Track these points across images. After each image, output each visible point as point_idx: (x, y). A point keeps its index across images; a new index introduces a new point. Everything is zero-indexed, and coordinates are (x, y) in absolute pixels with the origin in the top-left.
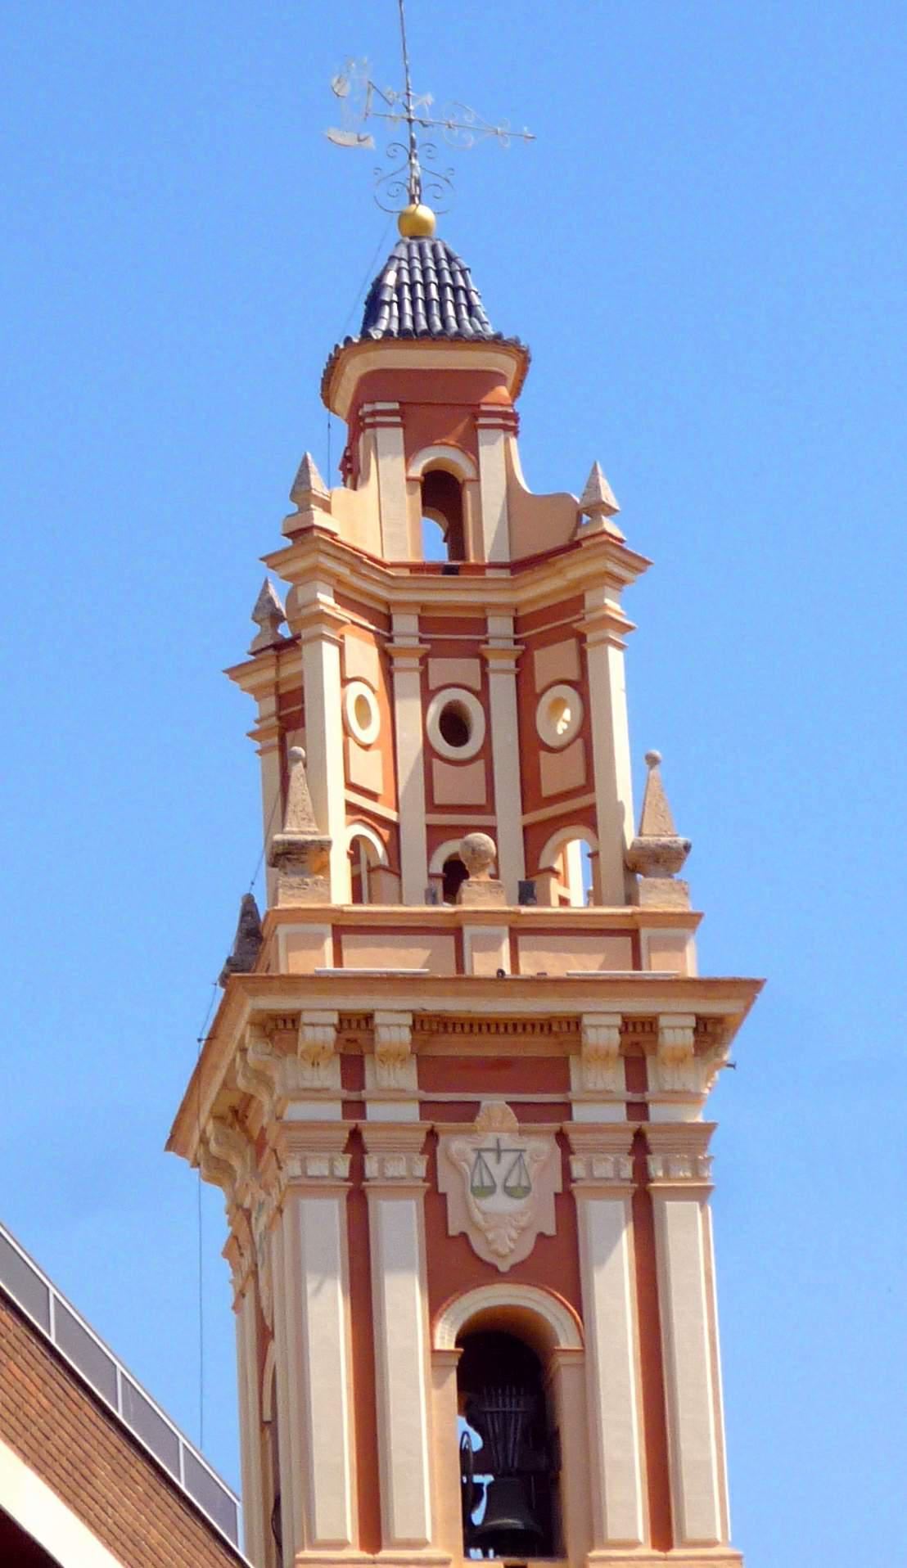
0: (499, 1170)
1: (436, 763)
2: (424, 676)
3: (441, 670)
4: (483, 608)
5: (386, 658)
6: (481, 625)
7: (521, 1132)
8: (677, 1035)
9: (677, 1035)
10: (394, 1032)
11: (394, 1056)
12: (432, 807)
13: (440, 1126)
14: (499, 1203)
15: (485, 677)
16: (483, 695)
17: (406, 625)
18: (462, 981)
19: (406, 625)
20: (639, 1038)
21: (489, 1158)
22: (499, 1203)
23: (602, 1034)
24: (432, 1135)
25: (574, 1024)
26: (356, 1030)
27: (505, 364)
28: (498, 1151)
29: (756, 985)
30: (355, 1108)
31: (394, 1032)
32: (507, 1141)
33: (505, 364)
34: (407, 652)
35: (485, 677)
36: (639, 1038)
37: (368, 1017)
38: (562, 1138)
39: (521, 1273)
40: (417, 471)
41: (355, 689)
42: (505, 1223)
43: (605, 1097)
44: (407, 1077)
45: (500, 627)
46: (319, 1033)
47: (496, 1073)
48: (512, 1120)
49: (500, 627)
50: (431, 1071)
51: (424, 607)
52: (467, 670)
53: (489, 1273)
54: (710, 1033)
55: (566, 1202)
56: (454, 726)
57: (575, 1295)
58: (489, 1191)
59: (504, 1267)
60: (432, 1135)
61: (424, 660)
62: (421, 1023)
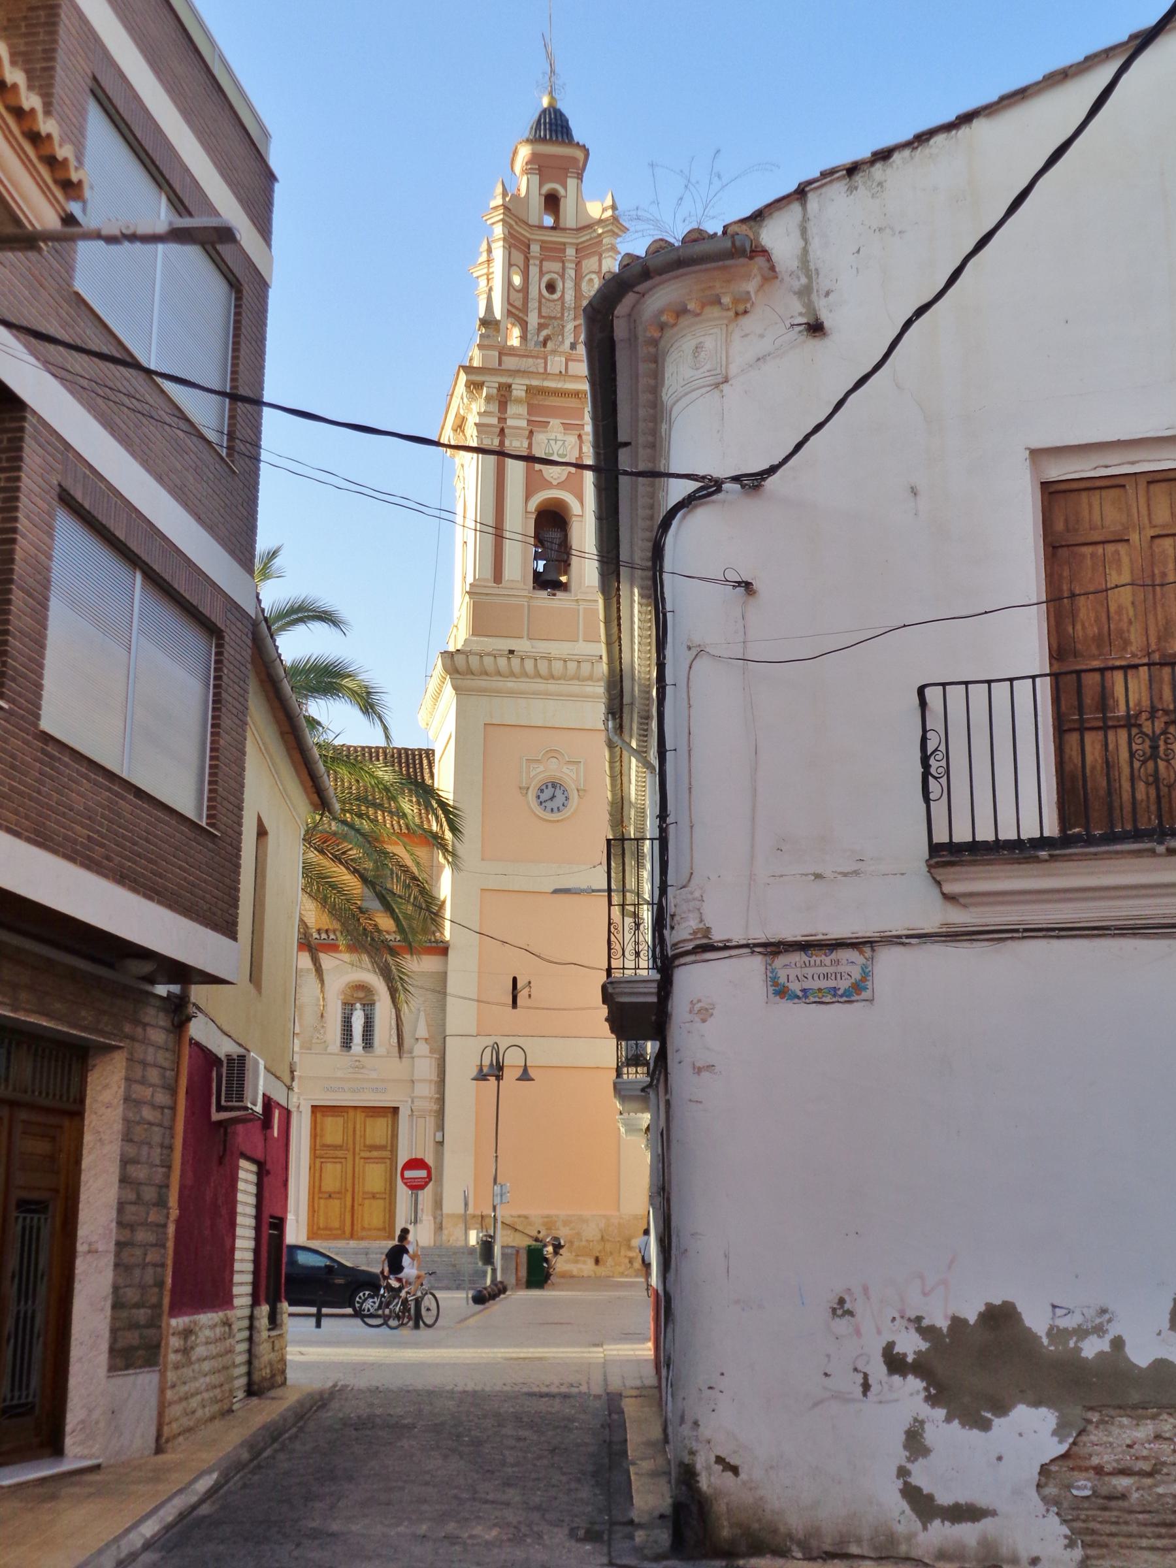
3: (547, 265)
4: (564, 244)
5: (527, 259)
6: (564, 250)
10: (518, 391)
11: (518, 401)
12: (540, 316)
16: (563, 276)
17: (535, 249)
18: (546, 374)
21: (552, 442)
24: (531, 432)
27: (580, 155)
28: (556, 440)
30: (502, 420)
32: (560, 437)
33: (580, 155)
34: (535, 258)
35: (564, 269)
37: (510, 386)
38: (580, 436)
40: (545, 190)
41: (514, 268)
44: (522, 410)
45: (571, 252)
49: (571, 252)
50: (532, 408)
51: (543, 242)
52: (556, 266)
56: (551, 287)
59: (555, 483)
60: (531, 432)
61: (541, 262)
62: (529, 389)
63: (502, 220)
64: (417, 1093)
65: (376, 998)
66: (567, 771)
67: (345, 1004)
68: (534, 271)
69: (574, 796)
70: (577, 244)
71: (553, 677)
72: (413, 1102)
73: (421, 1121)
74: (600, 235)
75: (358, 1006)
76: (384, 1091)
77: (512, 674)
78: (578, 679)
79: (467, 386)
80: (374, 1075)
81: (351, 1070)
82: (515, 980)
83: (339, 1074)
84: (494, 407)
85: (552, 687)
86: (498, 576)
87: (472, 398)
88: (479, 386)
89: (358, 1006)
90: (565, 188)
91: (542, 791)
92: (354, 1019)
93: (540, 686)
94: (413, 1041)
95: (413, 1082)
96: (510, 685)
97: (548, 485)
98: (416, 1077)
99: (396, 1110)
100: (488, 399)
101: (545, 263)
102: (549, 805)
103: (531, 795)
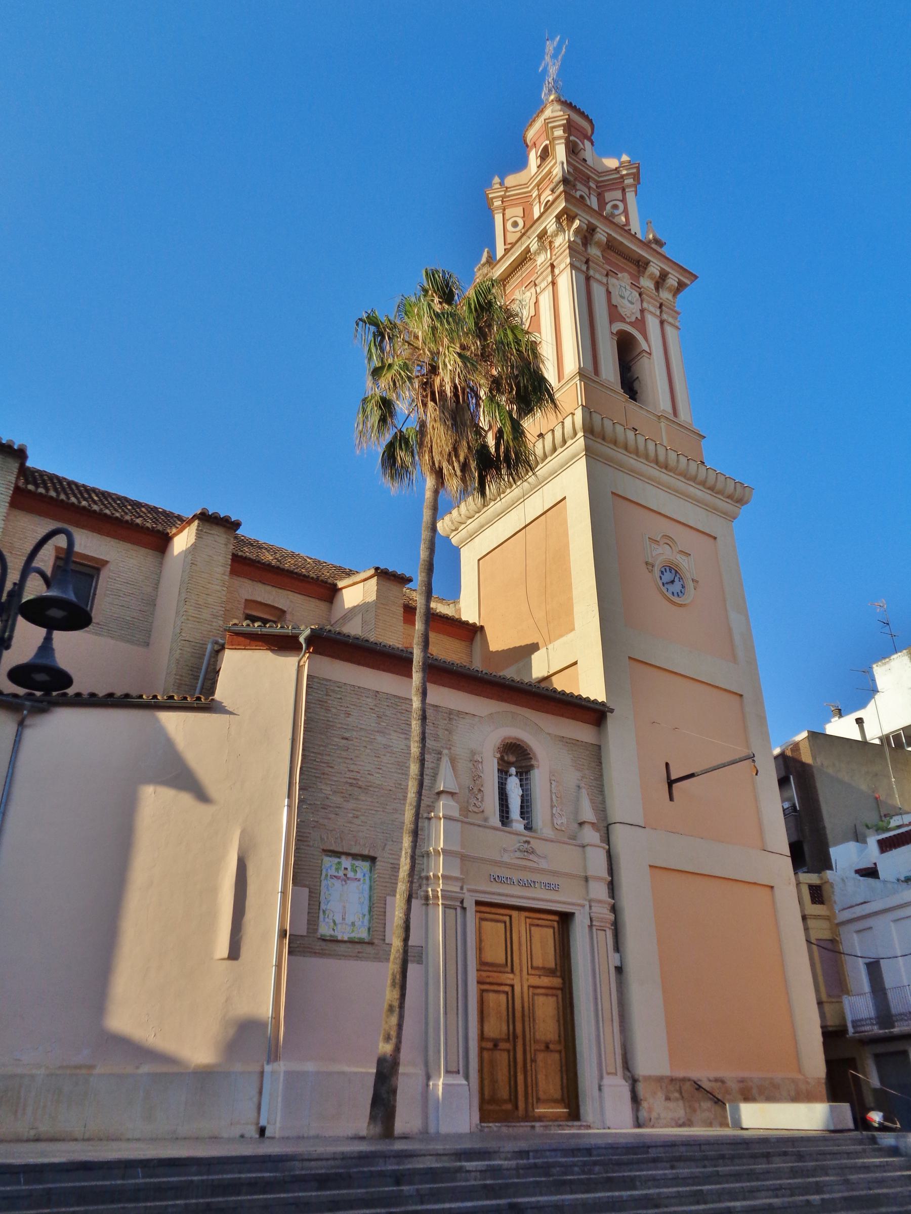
0: (626, 294)
8: (672, 281)
13: (611, 273)
20: (664, 276)
22: (626, 302)
23: (654, 269)
24: (607, 275)
25: (647, 263)
29: (696, 277)
32: (628, 287)
36: (664, 276)
38: (640, 295)
39: (630, 324)
42: (629, 307)
52: (586, 190)
53: (623, 320)
54: (681, 286)
55: (642, 311)
58: (623, 298)
62: (610, 239)
63: (563, 125)
64: (592, 895)
65: (533, 762)
69: (690, 585)
70: (598, 182)
71: (666, 468)
72: (590, 907)
73: (601, 933)
74: (622, 177)
75: (513, 770)
76: (554, 888)
77: (637, 452)
78: (685, 477)
79: (558, 217)
80: (543, 865)
81: (518, 854)
83: (506, 858)
85: (664, 477)
87: (560, 229)
88: (571, 219)
89: (513, 770)
91: (662, 573)
93: (654, 472)
94: (576, 826)
95: (586, 879)
97: (623, 320)
98: (589, 874)
99: (565, 919)
100: (577, 231)
102: (672, 588)
103: (657, 573)
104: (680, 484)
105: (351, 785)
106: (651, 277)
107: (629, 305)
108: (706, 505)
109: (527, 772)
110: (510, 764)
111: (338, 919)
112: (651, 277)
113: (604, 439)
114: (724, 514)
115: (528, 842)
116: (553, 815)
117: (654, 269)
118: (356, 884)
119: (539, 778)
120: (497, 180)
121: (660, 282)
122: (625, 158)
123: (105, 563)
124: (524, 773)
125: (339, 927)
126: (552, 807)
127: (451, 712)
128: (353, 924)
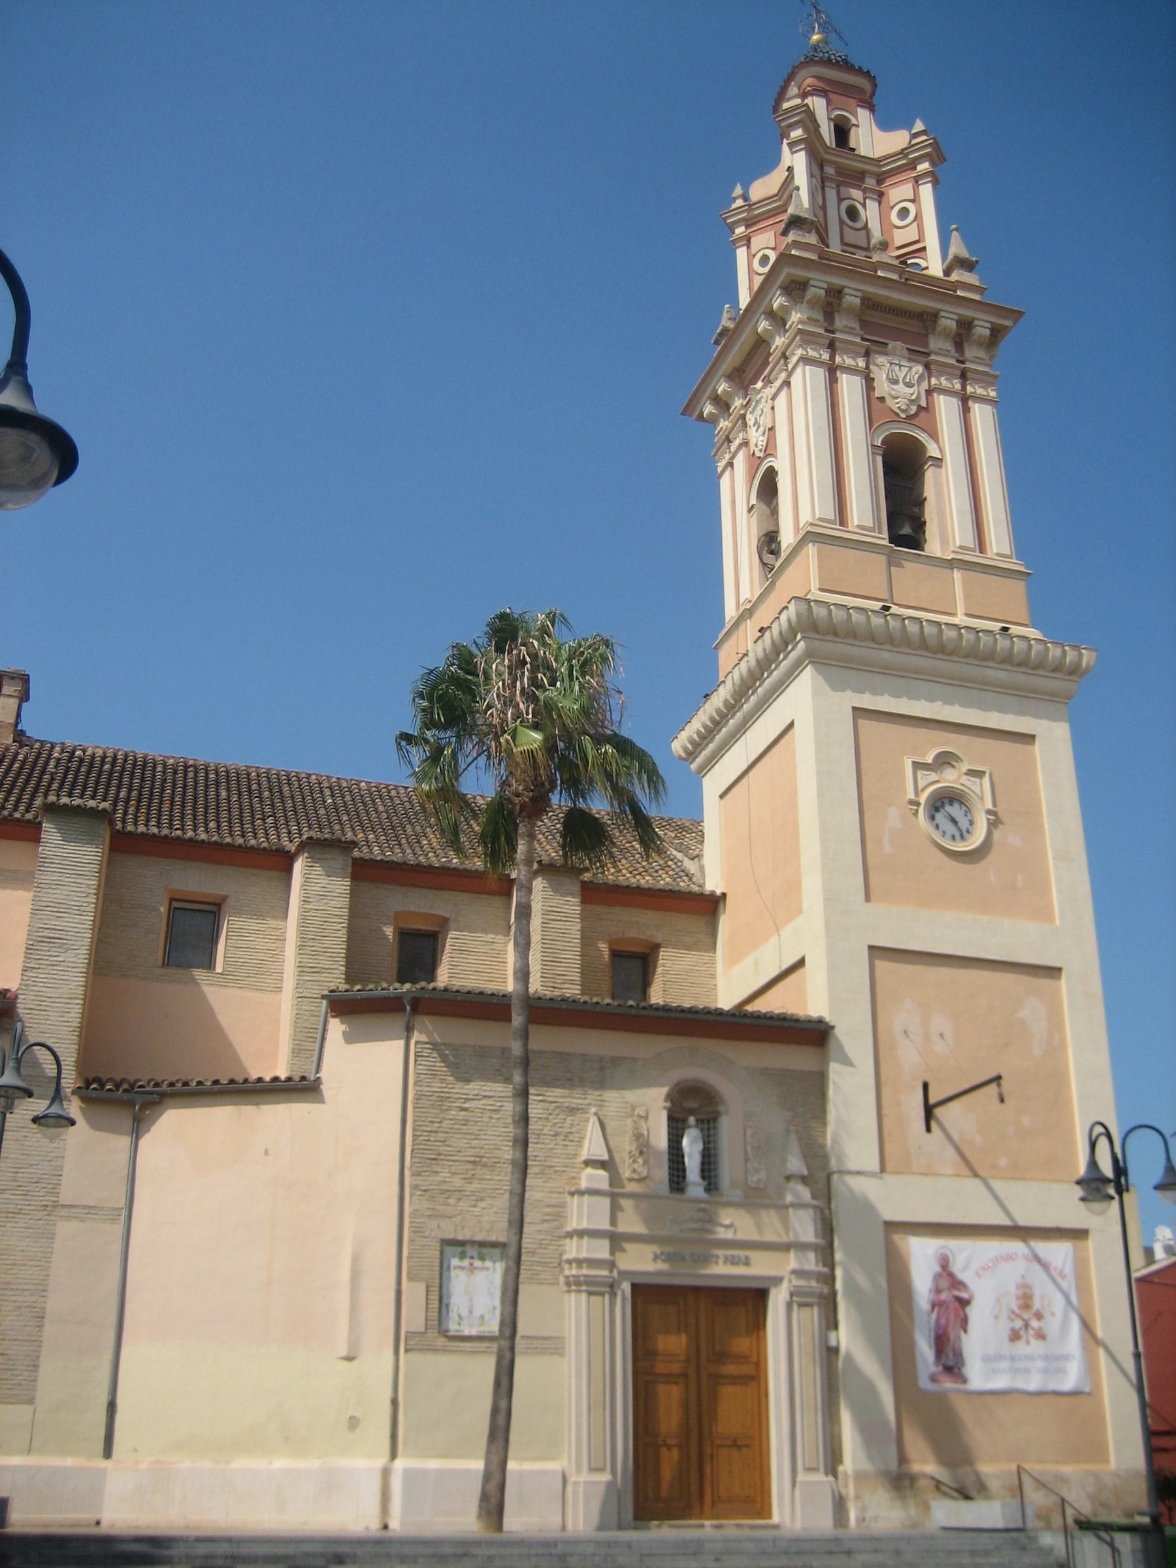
0: (901, 376)
1: (845, 228)
2: (838, 193)
7: (910, 360)
8: (982, 331)
9: (982, 331)
10: (852, 300)
14: (900, 387)
15: (865, 199)
17: (830, 170)
19: (830, 170)
20: (966, 325)
22: (900, 387)
23: (948, 323)
25: (935, 316)
26: (836, 293)
28: (900, 366)
29: (1021, 314)
31: (852, 300)
36: (966, 325)
43: (946, 353)
44: (855, 324)
46: (816, 291)
47: (897, 334)
48: (906, 352)
50: (864, 324)
54: (997, 333)
57: (934, 436)
58: (896, 382)
61: (838, 186)
65: (721, 1108)
66: (968, 783)
67: (671, 1119)
68: (831, 194)
70: (878, 175)
75: (692, 1120)
78: (976, 657)
80: (729, 1235)
82: (926, 1086)
84: (819, 316)
85: (942, 665)
86: (842, 518)
89: (692, 1120)
90: (855, 115)
92: (685, 1142)
96: (885, 655)
101: (843, 189)
104: (972, 671)
105: (474, 1163)
106: (945, 333)
107: (911, 390)
108: (1017, 689)
109: (715, 1120)
110: (691, 1112)
111: (464, 1313)
112: (945, 333)
113: (836, 634)
114: (1051, 695)
115: (704, 1210)
116: (746, 1170)
117: (948, 323)
118: (485, 1273)
119: (727, 1128)
120: (738, 191)
121: (962, 335)
122: (919, 126)
123: (225, 898)
124: (709, 1125)
125: (466, 1321)
126: (746, 1160)
127: (601, 1059)
128: (482, 1317)
